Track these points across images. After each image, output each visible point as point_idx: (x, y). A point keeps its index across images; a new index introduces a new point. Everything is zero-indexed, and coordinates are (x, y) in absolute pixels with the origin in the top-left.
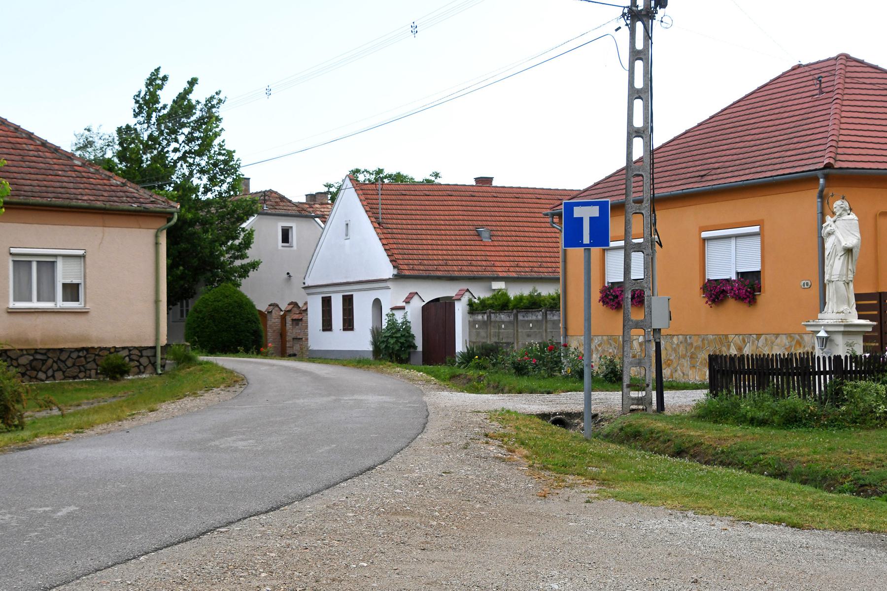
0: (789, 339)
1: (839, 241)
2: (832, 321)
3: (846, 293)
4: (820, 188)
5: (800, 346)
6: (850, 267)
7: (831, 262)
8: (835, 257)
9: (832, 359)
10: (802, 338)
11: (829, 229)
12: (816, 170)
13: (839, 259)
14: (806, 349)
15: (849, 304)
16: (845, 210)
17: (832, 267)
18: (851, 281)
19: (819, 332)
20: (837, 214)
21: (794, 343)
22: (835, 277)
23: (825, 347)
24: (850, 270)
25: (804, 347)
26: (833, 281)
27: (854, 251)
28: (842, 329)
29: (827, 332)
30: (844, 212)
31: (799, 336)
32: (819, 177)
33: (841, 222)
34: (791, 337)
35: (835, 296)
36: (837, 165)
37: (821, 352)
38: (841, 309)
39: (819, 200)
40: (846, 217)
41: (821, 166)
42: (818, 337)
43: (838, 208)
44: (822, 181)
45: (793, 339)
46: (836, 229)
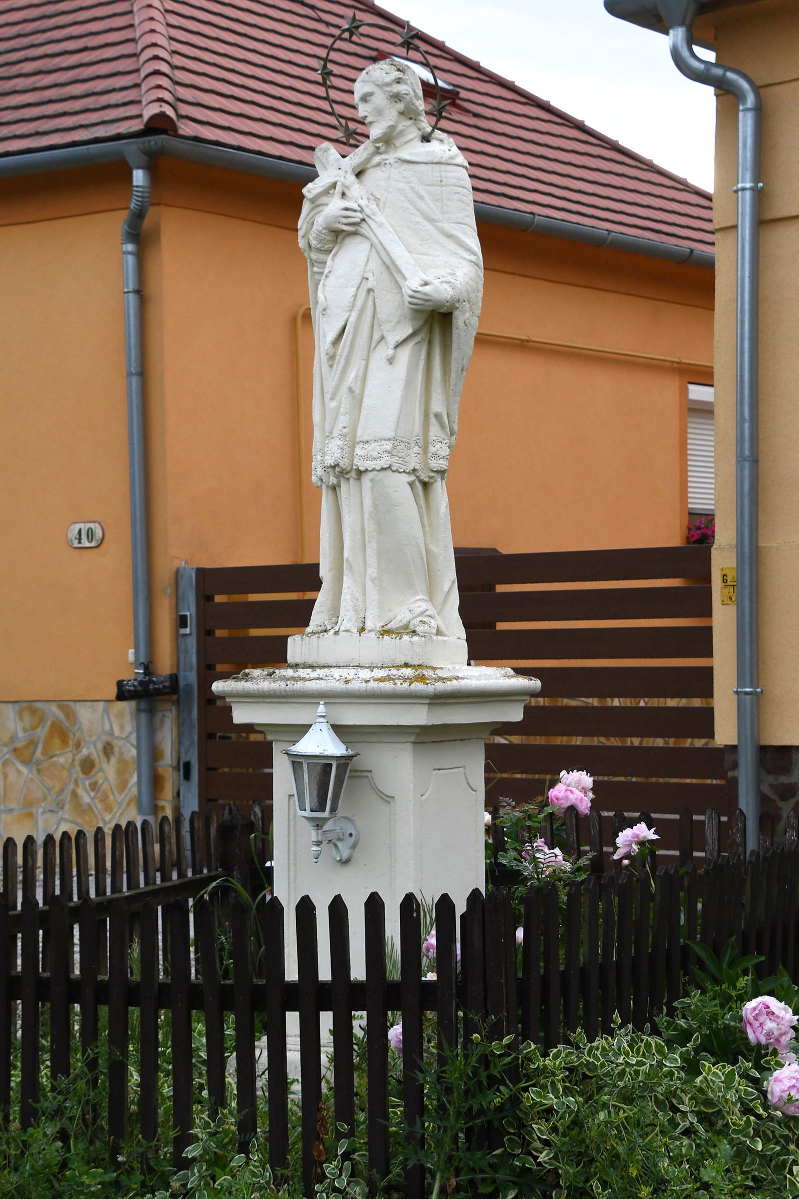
0: (27, 717)
1: (391, 269)
2: (365, 674)
3: (419, 534)
4: (132, 206)
5: (64, 741)
6: (437, 405)
7: (352, 375)
8: (370, 349)
9: (461, 908)
10: (70, 715)
11: (334, 206)
12: (118, 137)
13: (391, 361)
14: (85, 752)
15: (431, 595)
16: (409, 114)
17: (357, 397)
18: (442, 473)
19: (302, 729)
20: (375, 132)
21: (42, 732)
22: (374, 449)
23: (333, 809)
24: (438, 416)
25: (78, 745)
26: (360, 473)
27: (460, 319)
28: (419, 716)
29: (339, 730)
30: (405, 123)
31: (61, 707)
32: (131, 159)
33: (396, 172)
34: (33, 712)
35: (372, 548)
36: (186, 129)
37: (314, 835)
38: (401, 616)
39: (130, 247)
40: (415, 150)
41: (136, 126)
42: (297, 762)
43: (379, 99)
44: (139, 177)
45: (42, 720)
46: (370, 208)
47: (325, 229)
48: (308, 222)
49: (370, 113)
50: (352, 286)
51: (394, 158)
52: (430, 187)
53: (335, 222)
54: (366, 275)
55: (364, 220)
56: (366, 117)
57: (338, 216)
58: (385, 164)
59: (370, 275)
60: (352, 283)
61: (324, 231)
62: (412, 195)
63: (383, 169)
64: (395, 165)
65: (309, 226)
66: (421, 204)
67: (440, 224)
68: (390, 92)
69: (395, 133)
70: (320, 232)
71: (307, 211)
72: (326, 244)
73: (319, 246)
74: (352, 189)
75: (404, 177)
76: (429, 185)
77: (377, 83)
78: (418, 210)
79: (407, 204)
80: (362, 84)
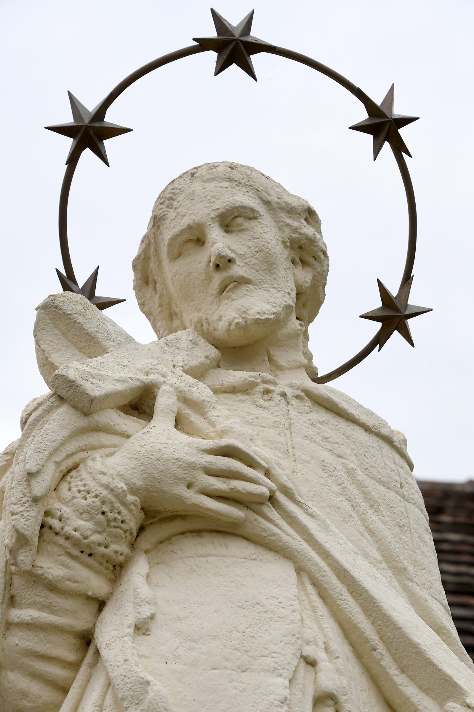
47: (134, 491)
48: (58, 464)
49: (242, 256)
50: (274, 671)
51: (291, 386)
52: (382, 489)
53: (177, 480)
54: (309, 651)
55: (272, 499)
56: (230, 261)
57: (192, 466)
58: (267, 392)
59: (320, 655)
60: (269, 661)
61: (131, 498)
62: (353, 489)
63: (261, 402)
64: (294, 402)
65: (58, 475)
66: (373, 518)
67: (416, 589)
68: (295, 230)
69: (285, 331)
70: (120, 497)
71: (65, 433)
72: (116, 538)
73: (96, 538)
74: (212, 414)
75: (326, 438)
76: (380, 481)
77: (270, 198)
78: (372, 532)
79: (346, 506)
80: (226, 184)
